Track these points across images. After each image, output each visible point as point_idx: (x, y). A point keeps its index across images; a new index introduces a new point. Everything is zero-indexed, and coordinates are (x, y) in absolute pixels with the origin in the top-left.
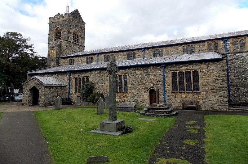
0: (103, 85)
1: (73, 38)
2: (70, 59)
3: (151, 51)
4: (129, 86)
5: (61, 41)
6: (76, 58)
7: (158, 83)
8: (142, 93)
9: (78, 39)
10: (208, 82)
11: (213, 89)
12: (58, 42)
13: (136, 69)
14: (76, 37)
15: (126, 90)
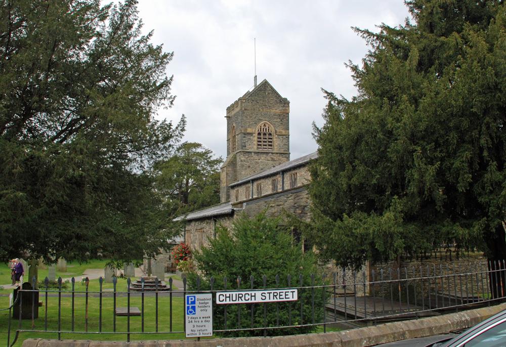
1: (256, 143)
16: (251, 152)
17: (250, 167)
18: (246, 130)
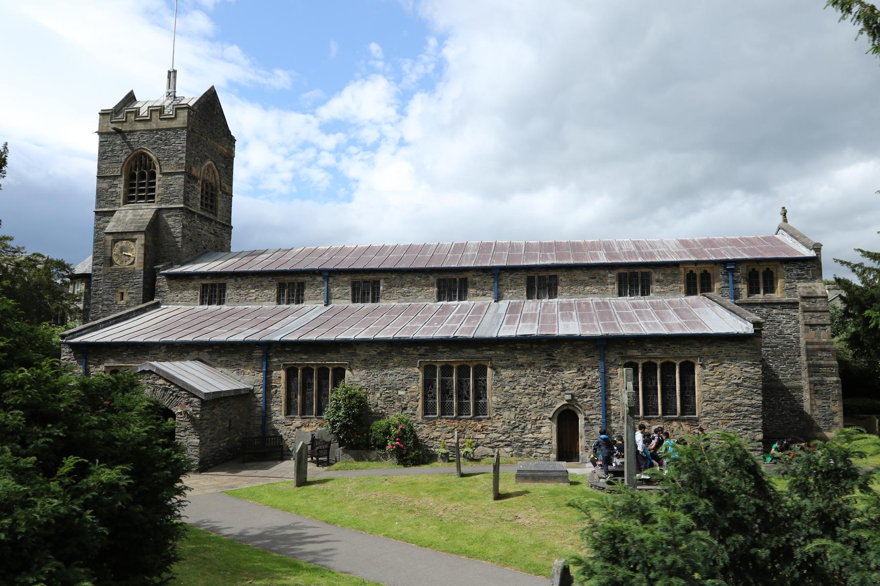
0: (400, 393)
1: (199, 196)
2: (204, 282)
3: (522, 279)
4: (494, 399)
5: (155, 206)
6: (232, 281)
7: (586, 390)
8: (536, 420)
9: (212, 201)
10: (717, 394)
11: (728, 411)
12: (145, 212)
13: (515, 349)
14: (207, 193)
15: (480, 410)
16: (193, 213)
17: (191, 240)
18: (191, 169)
